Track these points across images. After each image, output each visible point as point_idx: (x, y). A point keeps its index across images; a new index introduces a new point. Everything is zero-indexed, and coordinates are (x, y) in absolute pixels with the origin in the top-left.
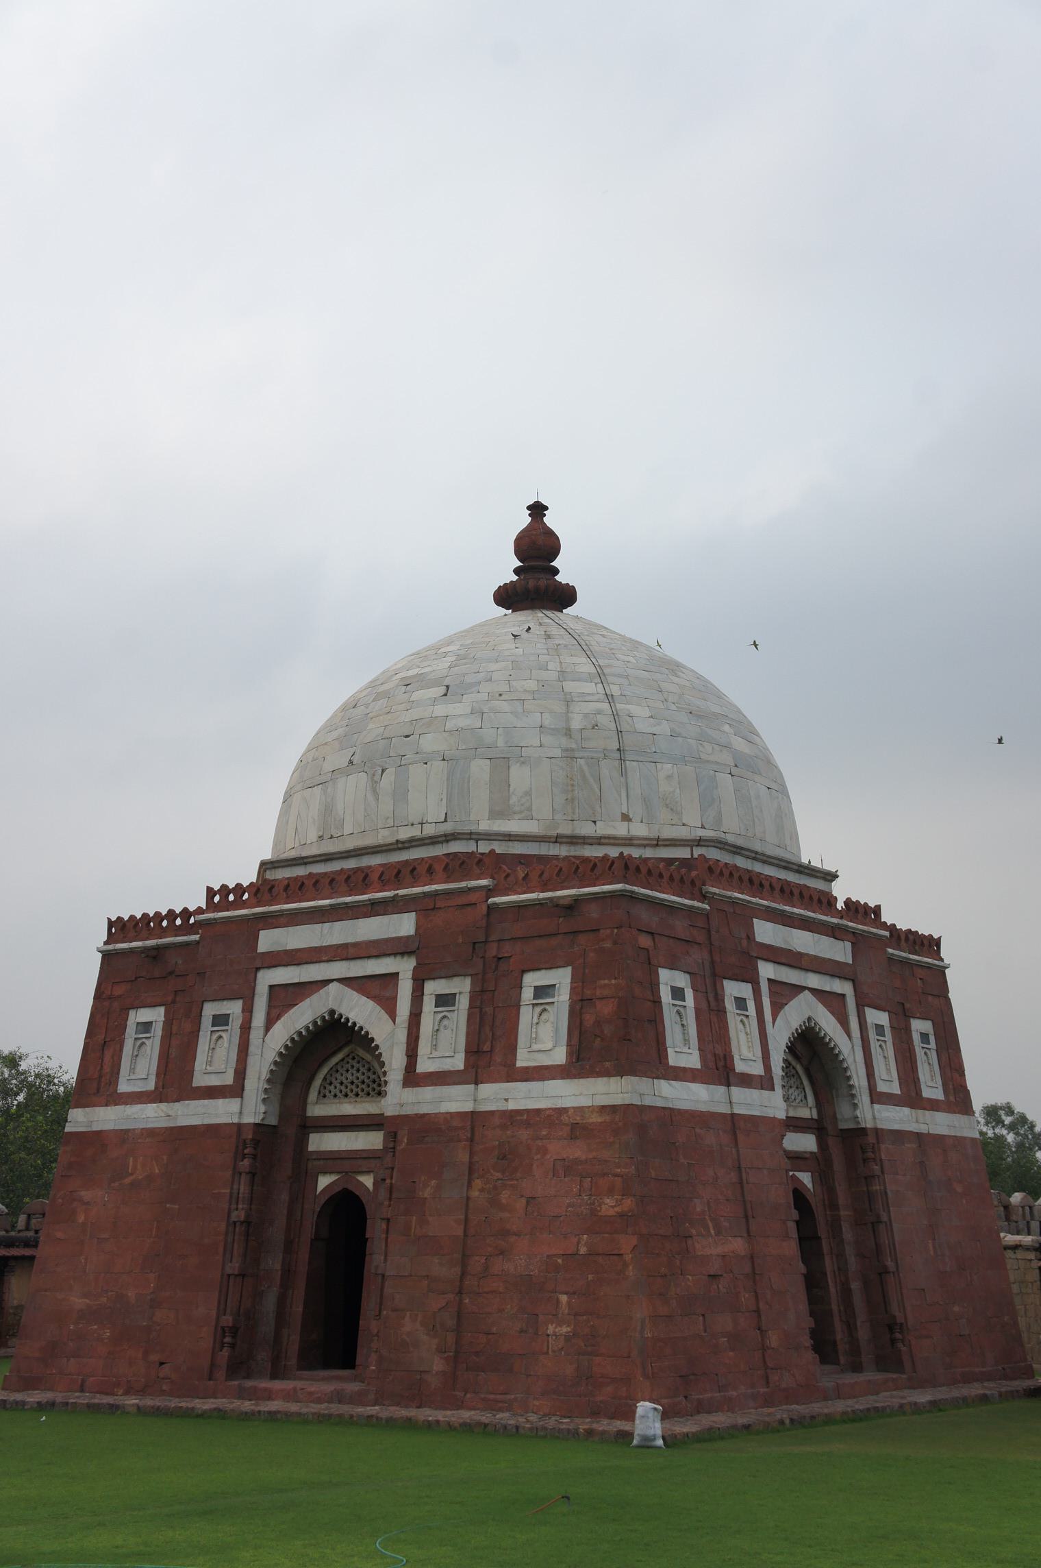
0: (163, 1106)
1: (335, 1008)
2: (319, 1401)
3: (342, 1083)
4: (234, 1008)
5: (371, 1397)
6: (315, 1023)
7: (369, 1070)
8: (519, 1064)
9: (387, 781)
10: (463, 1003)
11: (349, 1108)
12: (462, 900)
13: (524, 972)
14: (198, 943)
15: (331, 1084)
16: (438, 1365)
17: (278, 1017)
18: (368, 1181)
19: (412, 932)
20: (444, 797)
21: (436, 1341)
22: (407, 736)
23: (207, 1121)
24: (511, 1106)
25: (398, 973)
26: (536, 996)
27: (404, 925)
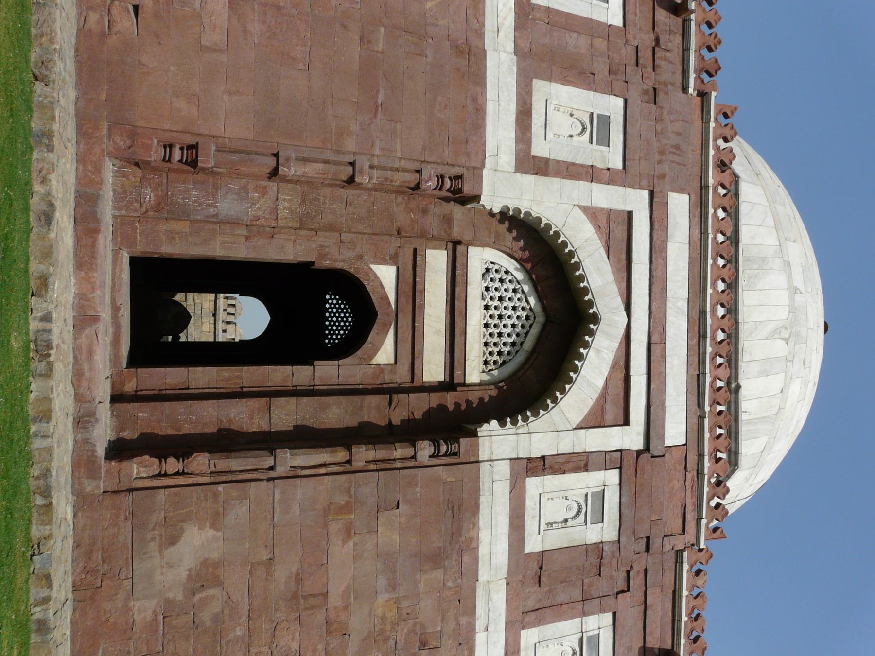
0: (509, 21)
1: (602, 326)
2: (78, 376)
3: (501, 299)
4: (614, 157)
5: (89, 486)
6: (586, 290)
7: (513, 344)
8: (524, 633)
9: (779, 348)
10: (593, 534)
11: (475, 316)
12: (690, 517)
13: (614, 614)
14: (685, 89)
15: (501, 281)
16: (143, 609)
17: (598, 228)
18: (385, 354)
19: (668, 443)
20: (752, 417)
21: (180, 597)
22: (804, 361)
23: (490, 107)
24: (480, 638)
25: (626, 422)
26: (589, 638)
27: (675, 431)
